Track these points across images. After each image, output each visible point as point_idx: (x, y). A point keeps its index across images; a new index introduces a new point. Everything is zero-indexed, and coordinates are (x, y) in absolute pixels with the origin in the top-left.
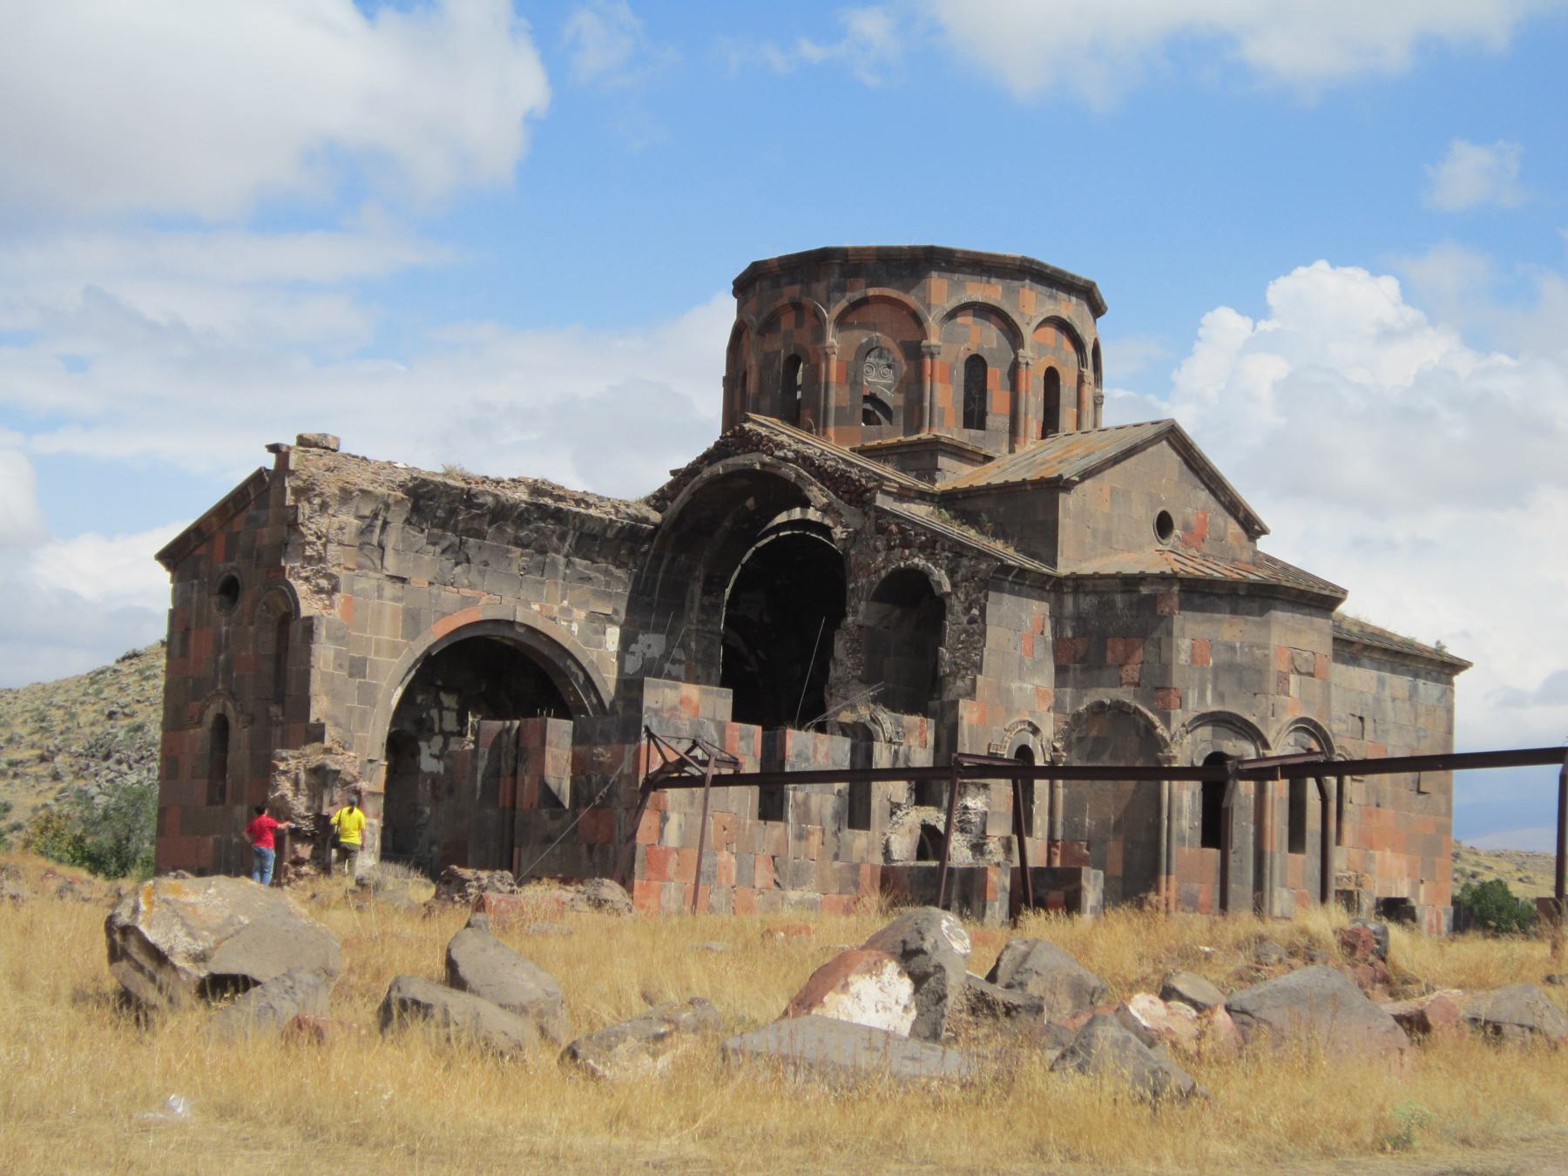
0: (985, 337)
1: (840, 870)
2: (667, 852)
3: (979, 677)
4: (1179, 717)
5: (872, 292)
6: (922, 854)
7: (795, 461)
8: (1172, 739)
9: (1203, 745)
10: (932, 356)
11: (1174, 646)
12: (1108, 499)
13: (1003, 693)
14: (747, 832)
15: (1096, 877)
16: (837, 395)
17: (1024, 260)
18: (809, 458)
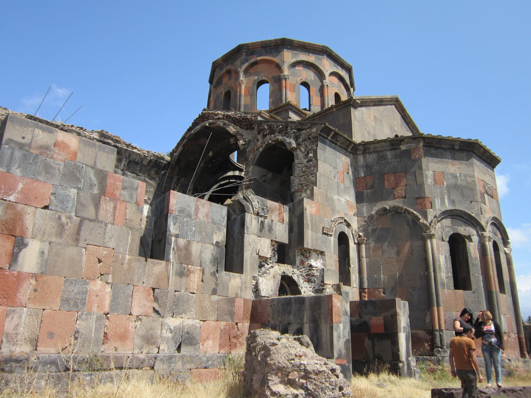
0: (309, 76)
1: (218, 302)
2: (20, 277)
3: (315, 187)
4: (431, 214)
5: (259, 58)
6: (282, 290)
7: (223, 119)
8: (430, 224)
9: (447, 229)
10: (285, 79)
11: (424, 174)
12: (373, 120)
13: (329, 201)
14: (126, 266)
15: (404, 306)
16: (244, 99)
17: (323, 46)
18: (229, 116)
